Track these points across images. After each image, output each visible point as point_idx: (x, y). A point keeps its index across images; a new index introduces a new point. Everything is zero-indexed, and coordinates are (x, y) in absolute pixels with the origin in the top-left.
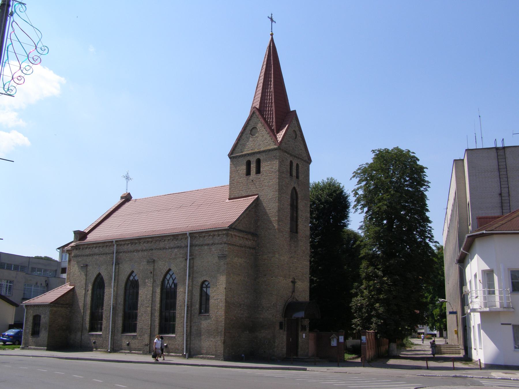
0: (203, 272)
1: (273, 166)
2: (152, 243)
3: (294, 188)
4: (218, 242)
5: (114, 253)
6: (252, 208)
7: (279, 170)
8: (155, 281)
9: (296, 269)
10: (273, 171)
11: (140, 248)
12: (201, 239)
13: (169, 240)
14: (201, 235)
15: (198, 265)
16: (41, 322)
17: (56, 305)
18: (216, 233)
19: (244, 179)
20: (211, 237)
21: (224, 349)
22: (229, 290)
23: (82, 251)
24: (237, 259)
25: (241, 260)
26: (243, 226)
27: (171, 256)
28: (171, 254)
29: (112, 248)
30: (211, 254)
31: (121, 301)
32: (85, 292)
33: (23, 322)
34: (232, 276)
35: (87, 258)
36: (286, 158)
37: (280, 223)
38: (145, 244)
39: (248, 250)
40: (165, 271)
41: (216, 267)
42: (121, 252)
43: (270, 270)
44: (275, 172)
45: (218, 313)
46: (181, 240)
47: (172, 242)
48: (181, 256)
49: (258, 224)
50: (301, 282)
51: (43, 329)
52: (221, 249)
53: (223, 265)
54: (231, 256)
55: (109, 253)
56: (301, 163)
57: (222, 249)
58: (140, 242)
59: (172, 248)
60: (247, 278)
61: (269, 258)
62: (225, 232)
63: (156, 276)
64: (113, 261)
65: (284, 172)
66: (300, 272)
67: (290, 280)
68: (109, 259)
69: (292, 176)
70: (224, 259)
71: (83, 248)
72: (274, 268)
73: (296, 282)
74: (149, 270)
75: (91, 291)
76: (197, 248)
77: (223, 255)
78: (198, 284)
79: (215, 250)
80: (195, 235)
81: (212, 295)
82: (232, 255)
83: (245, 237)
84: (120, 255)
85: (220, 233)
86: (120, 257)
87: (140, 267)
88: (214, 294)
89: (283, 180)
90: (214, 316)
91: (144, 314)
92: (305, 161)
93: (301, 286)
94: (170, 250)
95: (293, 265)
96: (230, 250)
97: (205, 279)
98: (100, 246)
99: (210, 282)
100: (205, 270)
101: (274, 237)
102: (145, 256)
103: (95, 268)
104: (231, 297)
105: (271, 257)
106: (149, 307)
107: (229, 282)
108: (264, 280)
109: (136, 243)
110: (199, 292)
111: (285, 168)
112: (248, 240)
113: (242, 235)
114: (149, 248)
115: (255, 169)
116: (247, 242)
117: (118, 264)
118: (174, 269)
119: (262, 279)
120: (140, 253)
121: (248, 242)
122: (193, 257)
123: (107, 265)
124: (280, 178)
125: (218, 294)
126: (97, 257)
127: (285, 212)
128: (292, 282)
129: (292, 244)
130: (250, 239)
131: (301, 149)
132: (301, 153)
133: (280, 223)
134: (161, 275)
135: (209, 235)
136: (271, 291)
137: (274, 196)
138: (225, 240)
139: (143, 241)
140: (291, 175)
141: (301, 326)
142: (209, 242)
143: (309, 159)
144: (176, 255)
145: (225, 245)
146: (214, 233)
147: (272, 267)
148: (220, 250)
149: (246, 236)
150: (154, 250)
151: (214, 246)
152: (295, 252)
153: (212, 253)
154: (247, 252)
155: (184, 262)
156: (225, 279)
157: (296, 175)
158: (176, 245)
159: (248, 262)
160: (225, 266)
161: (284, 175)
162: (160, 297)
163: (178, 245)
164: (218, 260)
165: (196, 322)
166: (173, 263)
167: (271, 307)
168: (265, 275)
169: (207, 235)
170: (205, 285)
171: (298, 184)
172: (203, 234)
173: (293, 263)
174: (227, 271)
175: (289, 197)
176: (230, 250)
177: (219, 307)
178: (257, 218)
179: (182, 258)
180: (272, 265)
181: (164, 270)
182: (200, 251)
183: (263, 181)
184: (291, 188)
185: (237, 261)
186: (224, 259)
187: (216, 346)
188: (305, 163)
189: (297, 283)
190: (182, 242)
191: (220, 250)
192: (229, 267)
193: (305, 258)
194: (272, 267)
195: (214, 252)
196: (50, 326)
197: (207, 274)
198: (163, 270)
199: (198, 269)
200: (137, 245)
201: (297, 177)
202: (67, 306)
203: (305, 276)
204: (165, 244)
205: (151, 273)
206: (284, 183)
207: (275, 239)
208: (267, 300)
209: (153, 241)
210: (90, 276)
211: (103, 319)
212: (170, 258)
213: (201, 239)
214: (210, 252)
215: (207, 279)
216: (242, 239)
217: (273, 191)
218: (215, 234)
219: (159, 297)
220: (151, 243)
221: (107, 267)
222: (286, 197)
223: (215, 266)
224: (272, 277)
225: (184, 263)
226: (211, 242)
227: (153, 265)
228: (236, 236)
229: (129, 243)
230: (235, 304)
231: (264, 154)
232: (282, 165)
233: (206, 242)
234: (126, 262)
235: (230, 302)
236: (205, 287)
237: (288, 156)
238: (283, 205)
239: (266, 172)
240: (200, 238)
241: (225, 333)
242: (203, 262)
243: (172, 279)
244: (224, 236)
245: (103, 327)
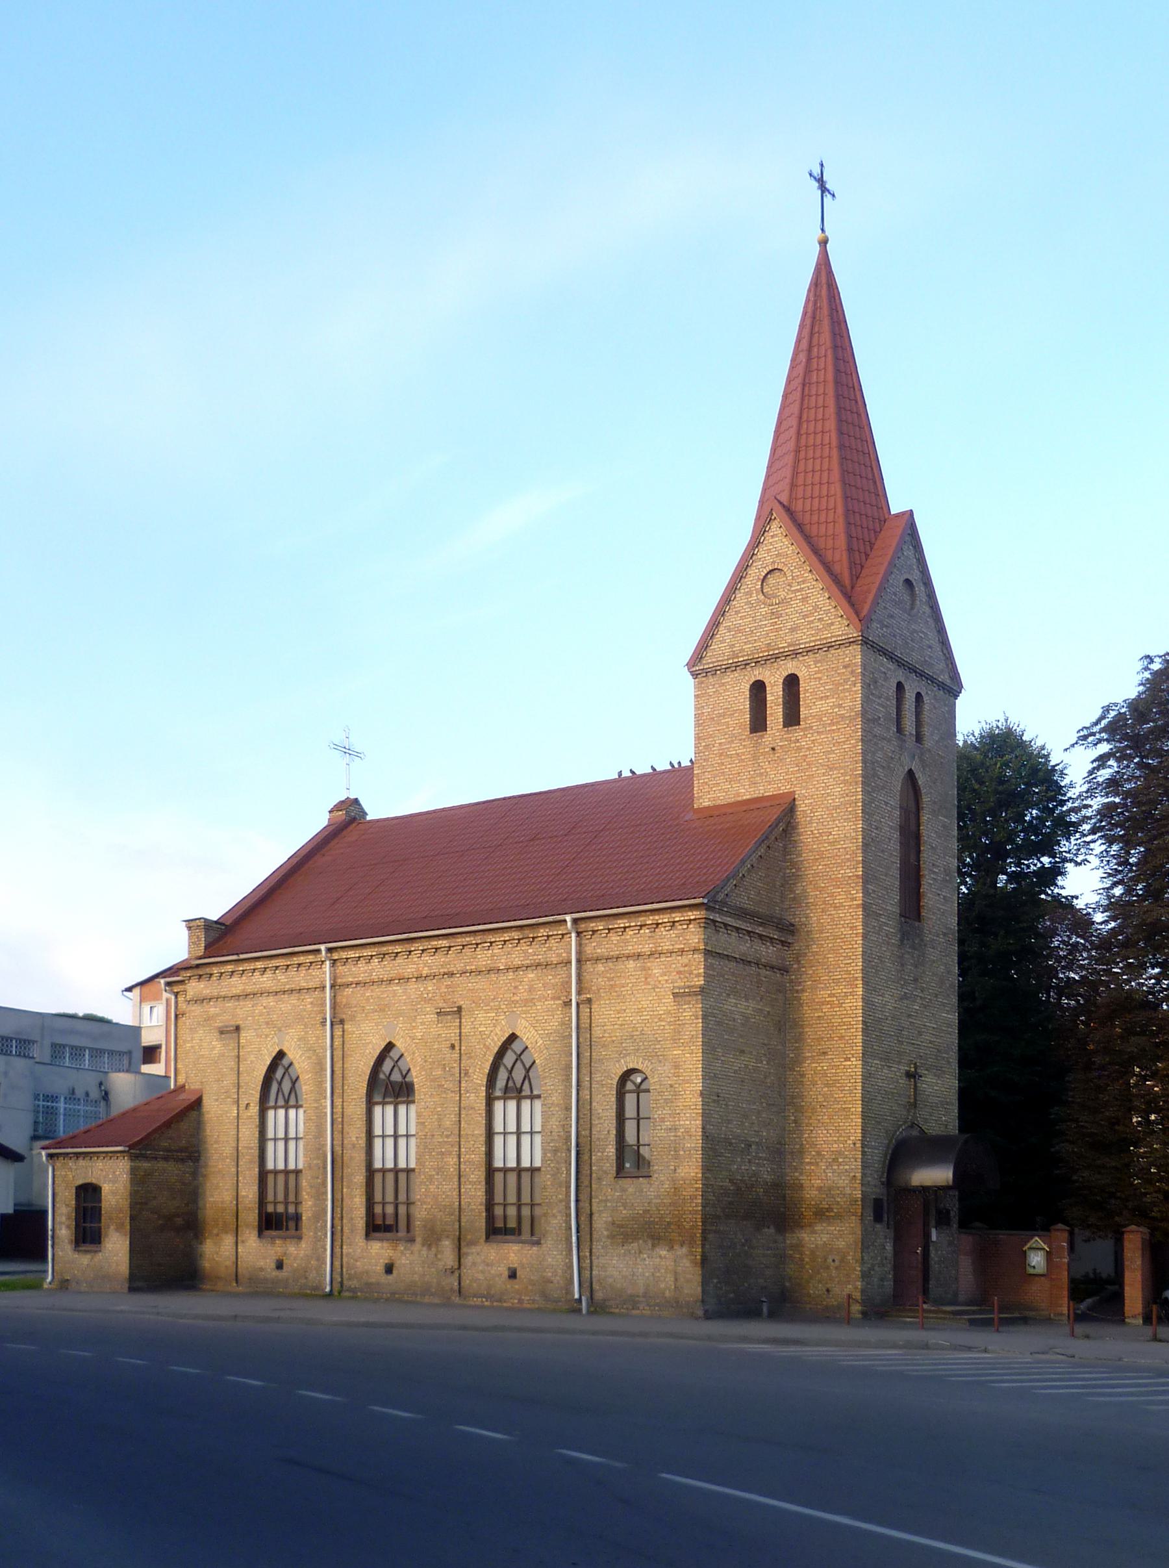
0: (624, 1045)
1: (842, 699)
2: (450, 952)
3: (911, 773)
4: (671, 947)
5: (324, 987)
6: (776, 838)
7: (864, 713)
8: (466, 1074)
9: (920, 1034)
10: (842, 717)
12: (614, 938)
13: (505, 941)
14: (613, 924)
15: (606, 1020)
16: (104, 1205)
17: (148, 1152)
18: (665, 918)
19: (742, 743)
20: (647, 931)
21: (704, 1283)
22: (714, 1101)
23: (219, 985)
24: (734, 1001)
25: (745, 1004)
26: (748, 898)
27: (514, 994)
28: (516, 987)
29: (314, 972)
30: (650, 987)
31: (357, 1138)
32: (238, 1110)
33: (47, 1207)
34: (720, 1054)
35: (237, 1004)
36: (885, 673)
37: (869, 886)
38: (426, 958)
39: (768, 972)
40: (499, 1040)
41: (667, 1027)
42: (348, 985)
43: (841, 1037)
44: (851, 719)
45: (678, 1171)
46: (546, 943)
47: (518, 948)
48: (549, 992)
49: (797, 892)
50: (935, 1076)
51: (112, 1227)
52: (682, 969)
53: (691, 1022)
54: (716, 993)
55: (308, 989)
56: (929, 692)
57: (686, 969)
58: (410, 952)
59: (518, 968)
60: (764, 1062)
61: (835, 999)
62: (695, 913)
63: (470, 1058)
64: (325, 1014)
65: (880, 718)
66: (930, 1045)
67: (900, 1067)
68: (309, 1006)
69: (905, 735)
70: (694, 1002)
71: (222, 973)
72: (852, 1030)
73: (921, 1076)
74: (446, 1041)
75: (258, 1108)
76: (600, 967)
77: (689, 987)
78: (609, 1081)
80: (594, 924)
81: (656, 1116)
82: (718, 990)
83: (757, 931)
84: (346, 993)
85: (677, 919)
86: (344, 1000)
87: (414, 1031)
88: (664, 1112)
89: (876, 744)
90: (668, 1180)
91: (436, 1177)
92: (942, 686)
93: (935, 1088)
94: (511, 974)
95: (911, 1022)
96: (711, 972)
97: (631, 1066)
98: (277, 967)
99: (648, 1073)
100: (633, 1036)
101: (851, 932)
102: (428, 994)
104: (720, 1121)
105: (843, 994)
106: (450, 1153)
107: (712, 1075)
108: (819, 1068)
109: (397, 953)
110: (615, 1106)
111: (883, 707)
112: (767, 941)
113: (748, 925)
114: (442, 971)
115: (781, 710)
116: (763, 948)
117: (342, 1022)
118: (528, 1035)
119: (814, 1065)
120: (412, 986)
121: (767, 948)
122: (588, 996)
123: (306, 1026)
124: (868, 739)
125: (677, 1112)
127: (883, 851)
128: (909, 1075)
129: (906, 956)
130: (772, 939)
131: (930, 647)
132: (930, 657)
133: (869, 886)
134: (485, 1056)
135: (639, 924)
136: (845, 1104)
137: (847, 799)
138: (697, 941)
139: (421, 948)
140: (900, 730)
141: (934, 1213)
142: (640, 946)
143: (952, 678)
144: (531, 990)
145: (695, 956)
146: (657, 917)
147: (845, 1027)
148: (679, 973)
149: (761, 929)
150: (458, 975)
151: (658, 960)
152: (916, 980)
153: (652, 983)
154: (764, 979)
155: (559, 1013)
156: (700, 1066)
157: (915, 733)
158: (531, 958)
159: (769, 1012)
160: (697, 1023)
161: (877, 730)
162: (486, 1124)
163: (535, 957)
164: (672, 1004)
165: (606, 1201)
166: (524, 1016)
167: (846, 1153)
168: (825, 1053)
169: (633, 924)
170: (634, 1083)
171: (922, 760)
172: (621, 921)
173: (909, 1016)
174: (705, 1040)
175: (895, 801)
176: (711, 972)
177: (682, 1153)
178: (794, 870)
179: (554, 998)
180: (844, 1020)
181: (496, 1039)
182: (612, 975)
183: (809, 749)
184: (901, 773)
185: (733, 1009)
186: (694, 1002)
187: (675, 1272)
188: (941, 692)
189: (923, 1079)
190: (550, 949)
191: (679, 973)
192: (710, 1026)
193: (944, 1001)
194: (845, 1027)
195: (660, 978)
196: (132, 1218)
197: (638, 1049)
198: (493, 1040)
199: (606, 1035)
200: (399, 960)
201: (919, 738)
202: (183, 1154)
203: (944, 1055)
204: (493, 956)
205: (453, 1047)
206: (879, 754)
207: (855, 939)
208: (831, 1131)
209: (455, 948)
210: (252, 1062)
212: (512, 999)
213: (613, 938)
214: (646, 979)
215: (640, 1067)
216: (748, 938)
217: (845, 782)
218: (660, 921)
219: (484, 1122)
220: (447, 954)
221: (307, 1033)
222: (886, 804)
223: (663, 1023)
224: (847, 1059)
225: (561, 1016)
226: (646, 949)
227: (458, 1024)
228: (729, 928)
229: (374, 953)
230: (731, 1144)
232: (872, 694)
233: (630, 949)
234: (366, 1016)
235: (716, 1135)
236: (630, 1092)
237: (891, 666)
238: (877, 829)
239: (821, 720)
240: (611, 935)
241: (704, 1232)
242: (625, 1010)
243: (524, 1065)
244: (691, 926)
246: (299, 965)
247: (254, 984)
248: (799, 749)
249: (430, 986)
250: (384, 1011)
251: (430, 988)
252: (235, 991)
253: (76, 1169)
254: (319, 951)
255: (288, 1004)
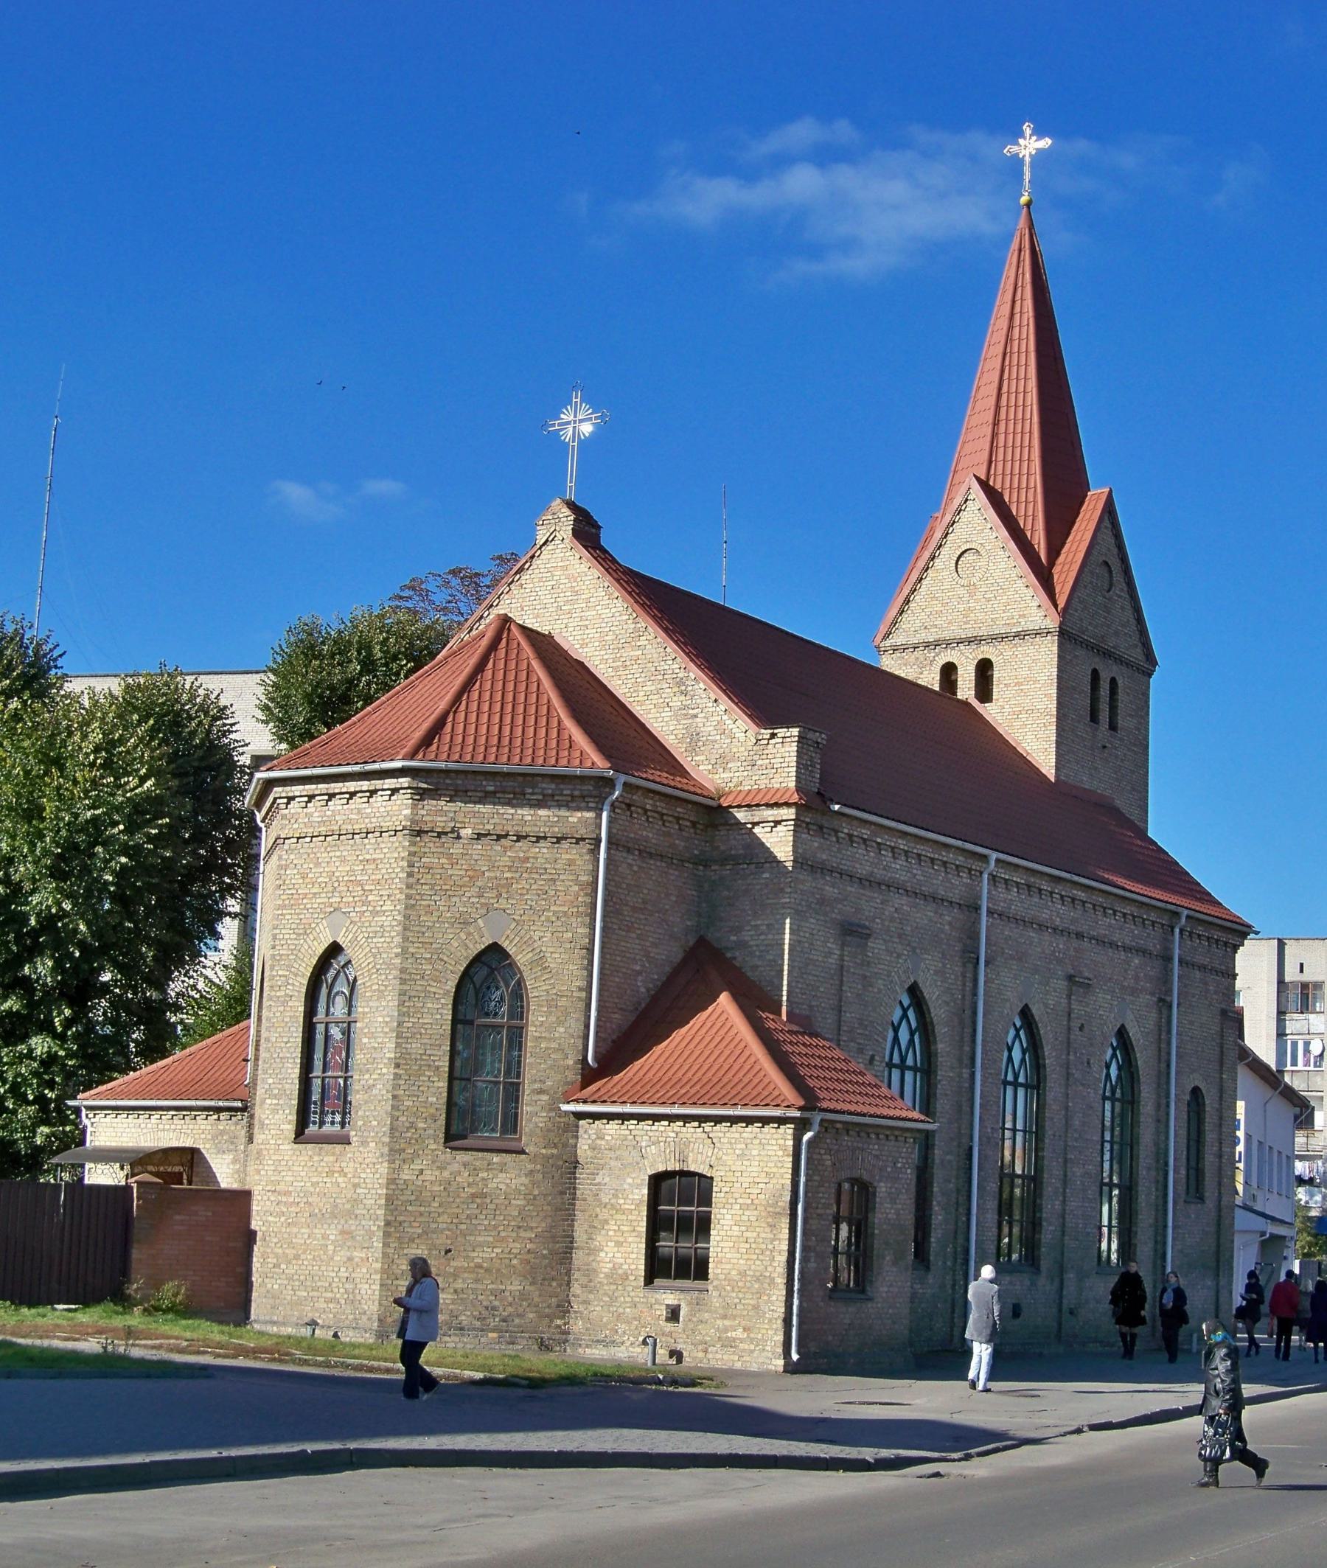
11: (1045, 915)
28: (1126, 971)
68: (947, 927)
79: (1216, 993)
103: (899, 956)
120: (1046, 936)
123: (944, 956)
126: (901, 901)
144: (1137, 978)
205: (1081, 1028)
211: (935, 1203)
231: (1124, 669)
245: (933, 1240)
246: (945, 863)
247: (884, 869)
248: (1117, 757)
249: (1061, 943)
250: (1020, 959)
251: (1061, 946)
252: (863, 870)
253: (838, 1151)
254: (985, 858)
255: (924, 915)
